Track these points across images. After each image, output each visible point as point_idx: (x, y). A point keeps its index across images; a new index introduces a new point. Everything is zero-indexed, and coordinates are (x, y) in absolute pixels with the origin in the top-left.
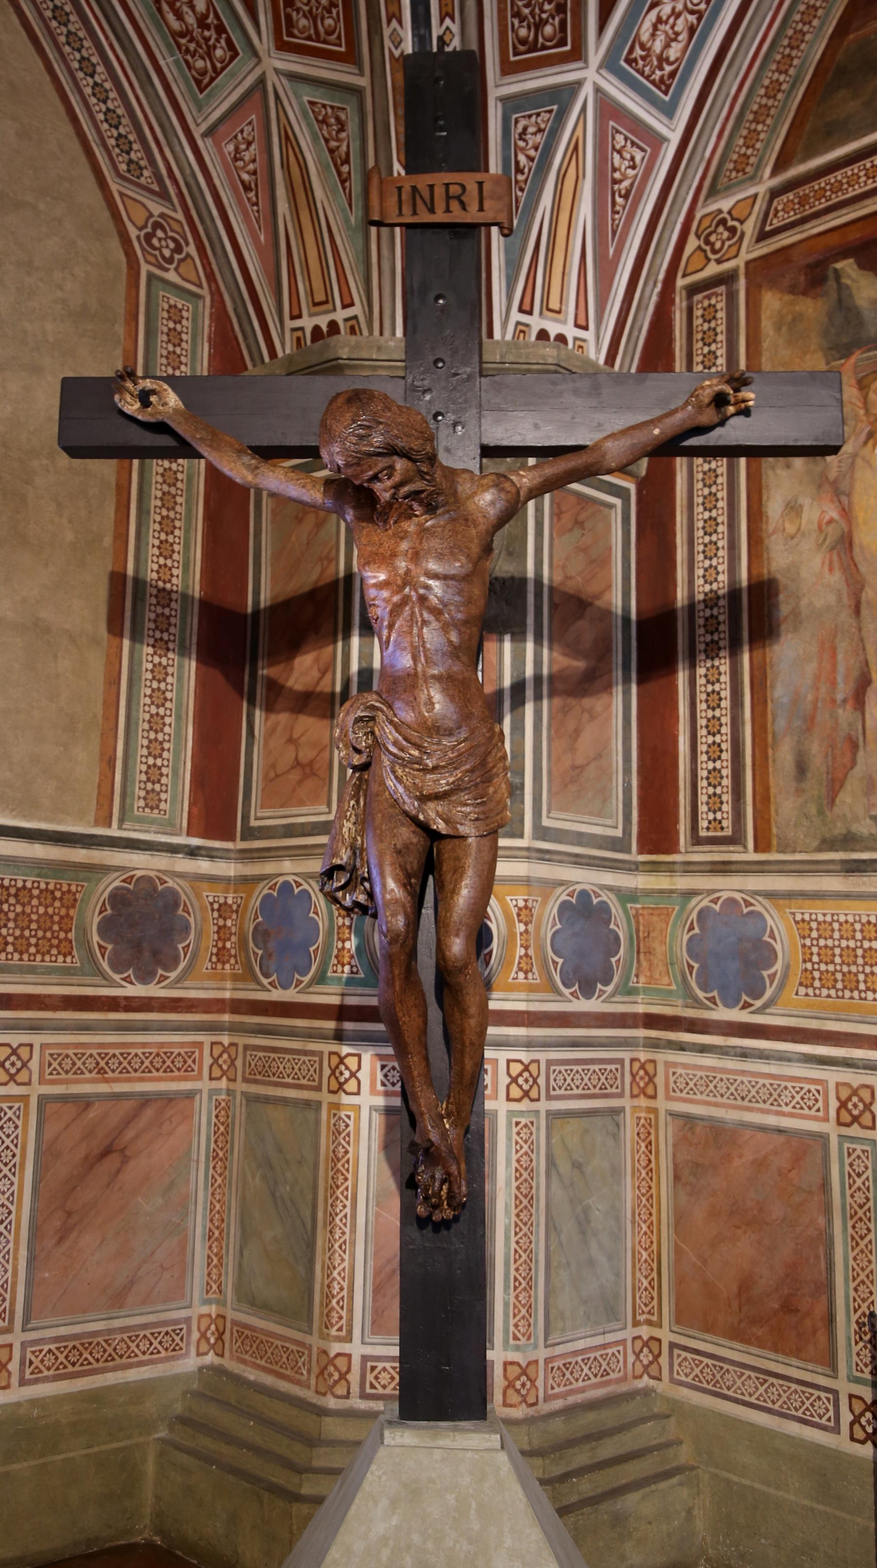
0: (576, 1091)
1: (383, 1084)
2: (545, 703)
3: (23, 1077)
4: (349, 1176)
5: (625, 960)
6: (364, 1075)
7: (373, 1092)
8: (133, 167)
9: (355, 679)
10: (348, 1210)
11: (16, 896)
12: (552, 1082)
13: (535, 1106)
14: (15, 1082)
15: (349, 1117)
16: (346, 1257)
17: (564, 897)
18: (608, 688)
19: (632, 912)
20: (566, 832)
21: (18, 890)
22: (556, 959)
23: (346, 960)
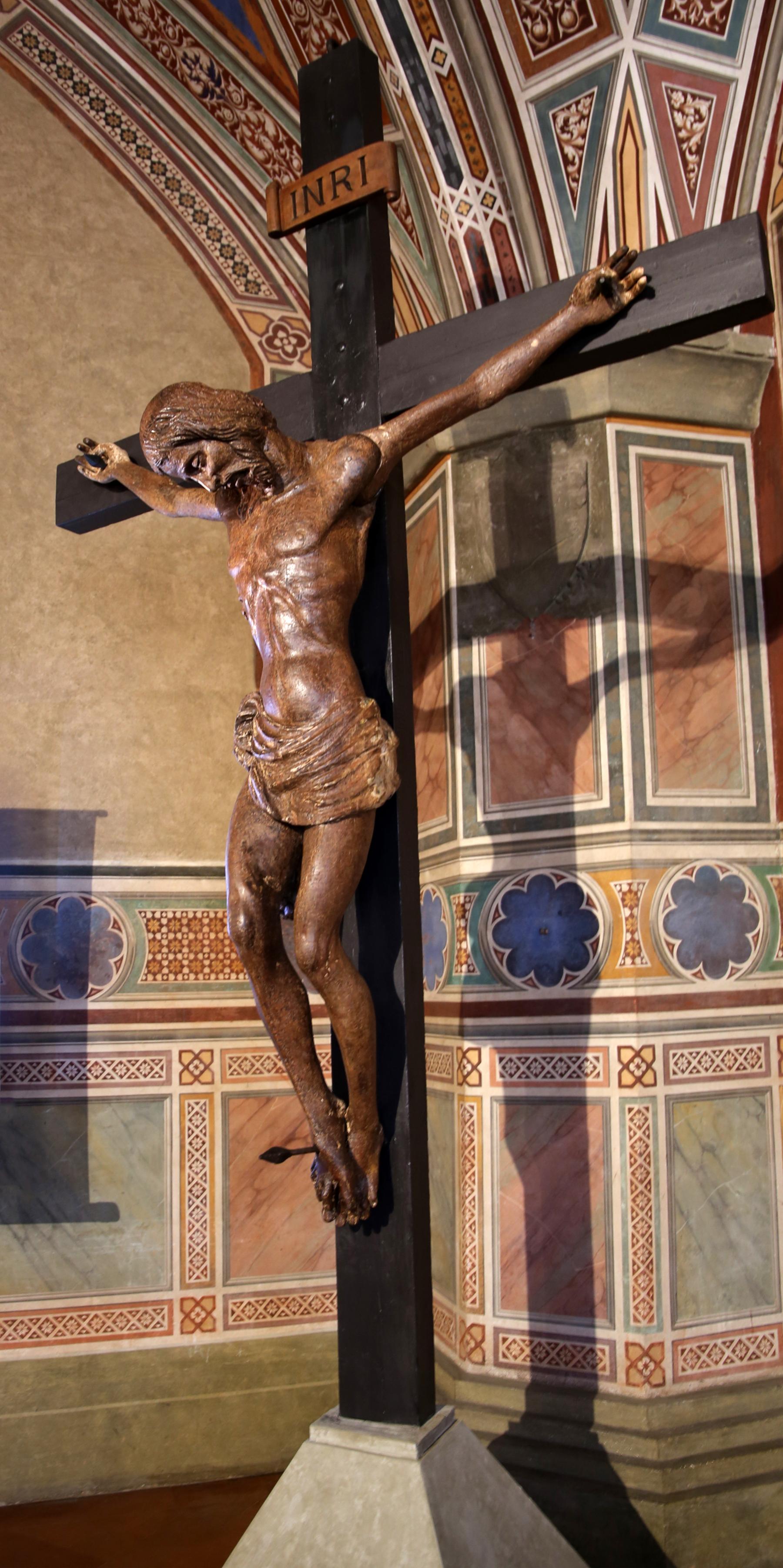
0: (703, 1074)
1: (502, 1076)
2: (644, 680)
3: (206, 1077)
4: (476, 1162)
5: (766, 935)
6: (484, 1068)
7: (493, 1083)
8: (249, 286)
9: (457, 690)
10: (476, 1194)
11: (188, 925)
12: (672, 1066)
13: (650, 1091)
14: (200, 1082)
15: (472, 1107)
16: (476, 1236)
17: (679, 876)
18: (729, 652)
19: (773, 884)
20: (681, 809)
21: (190, 920)
22: (671, 940)
23: (463, 959)
